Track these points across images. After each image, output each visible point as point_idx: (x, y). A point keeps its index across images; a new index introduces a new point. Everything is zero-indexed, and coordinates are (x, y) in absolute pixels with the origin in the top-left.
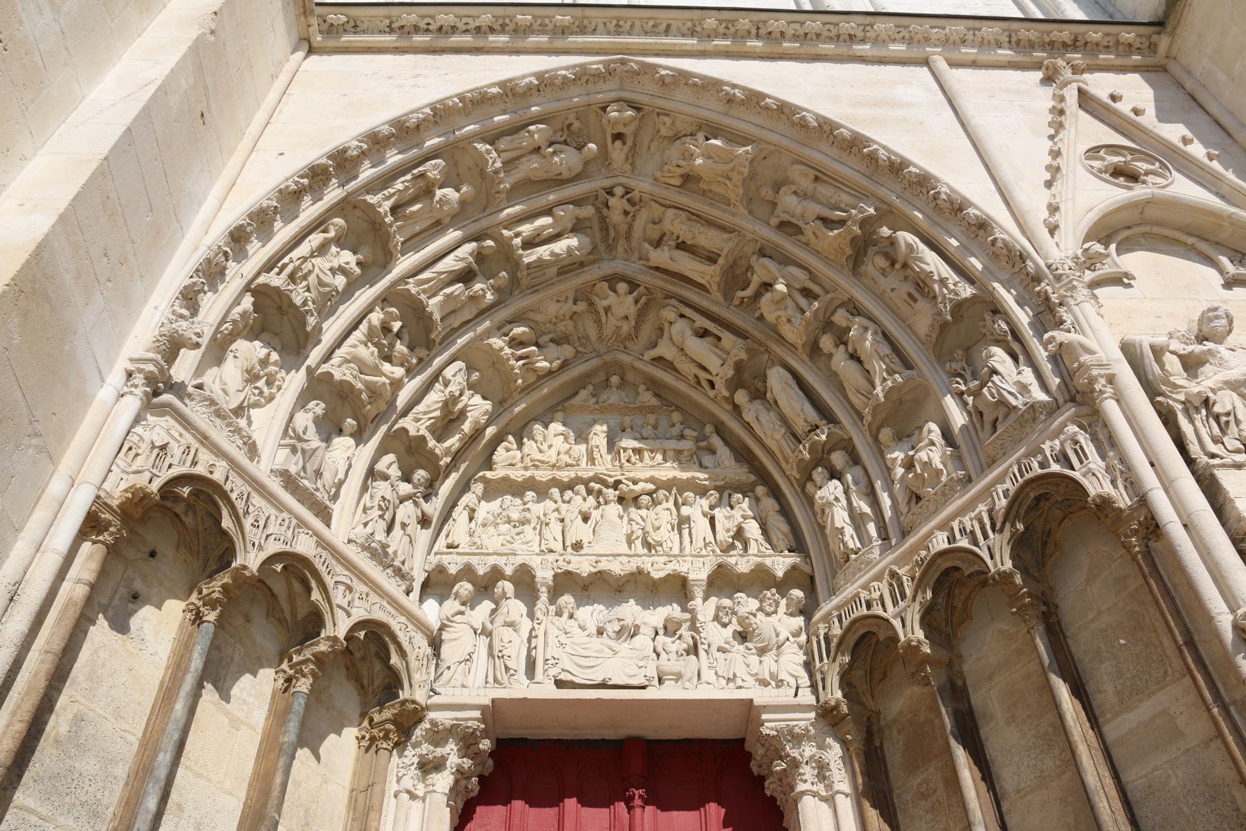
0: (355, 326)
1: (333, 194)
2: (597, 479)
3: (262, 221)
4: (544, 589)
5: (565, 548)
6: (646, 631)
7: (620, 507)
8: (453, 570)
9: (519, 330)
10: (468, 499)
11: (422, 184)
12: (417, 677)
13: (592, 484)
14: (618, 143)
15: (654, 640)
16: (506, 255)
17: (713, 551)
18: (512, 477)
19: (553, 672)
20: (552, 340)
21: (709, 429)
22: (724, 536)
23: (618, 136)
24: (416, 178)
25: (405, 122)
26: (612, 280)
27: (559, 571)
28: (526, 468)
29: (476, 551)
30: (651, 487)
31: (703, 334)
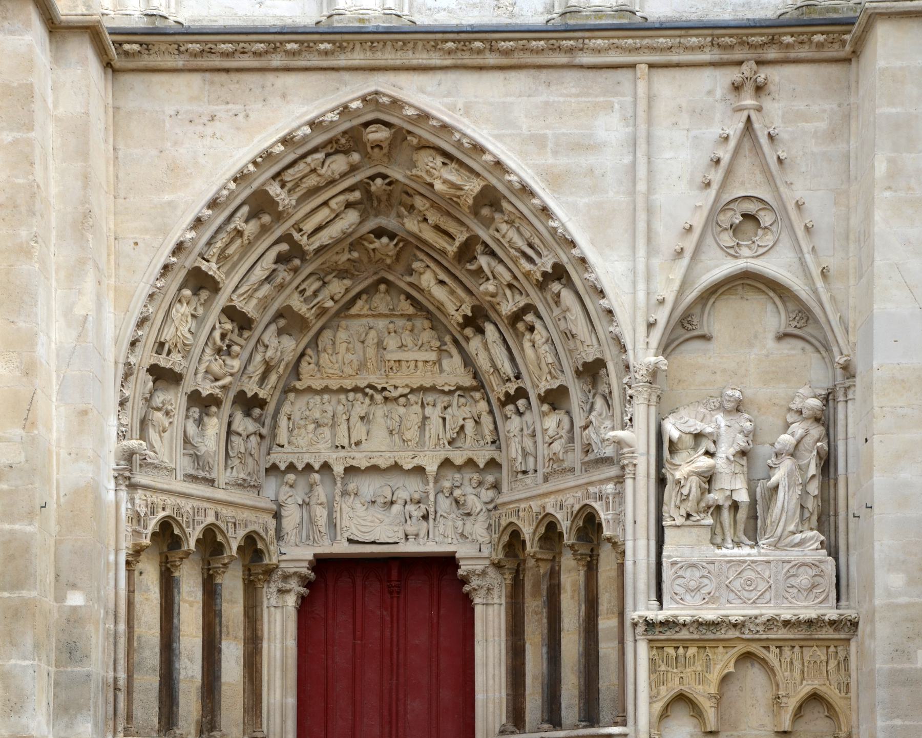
2: (370, 386)
4: (339, 479)
5: (350, 445)
6: (401, 502)
7: (385, 408)
8: (283, 467)
13: (367, 390)
15: (404, 506)
17: (444, 444)
18: (314, 387)
19: (346, 535)
21: (448, 339)
22: (451, 434)
26: (379, 233)
27: (348, 465)
29: (296, 450)
30: (407, 391)
31: (442, 282)
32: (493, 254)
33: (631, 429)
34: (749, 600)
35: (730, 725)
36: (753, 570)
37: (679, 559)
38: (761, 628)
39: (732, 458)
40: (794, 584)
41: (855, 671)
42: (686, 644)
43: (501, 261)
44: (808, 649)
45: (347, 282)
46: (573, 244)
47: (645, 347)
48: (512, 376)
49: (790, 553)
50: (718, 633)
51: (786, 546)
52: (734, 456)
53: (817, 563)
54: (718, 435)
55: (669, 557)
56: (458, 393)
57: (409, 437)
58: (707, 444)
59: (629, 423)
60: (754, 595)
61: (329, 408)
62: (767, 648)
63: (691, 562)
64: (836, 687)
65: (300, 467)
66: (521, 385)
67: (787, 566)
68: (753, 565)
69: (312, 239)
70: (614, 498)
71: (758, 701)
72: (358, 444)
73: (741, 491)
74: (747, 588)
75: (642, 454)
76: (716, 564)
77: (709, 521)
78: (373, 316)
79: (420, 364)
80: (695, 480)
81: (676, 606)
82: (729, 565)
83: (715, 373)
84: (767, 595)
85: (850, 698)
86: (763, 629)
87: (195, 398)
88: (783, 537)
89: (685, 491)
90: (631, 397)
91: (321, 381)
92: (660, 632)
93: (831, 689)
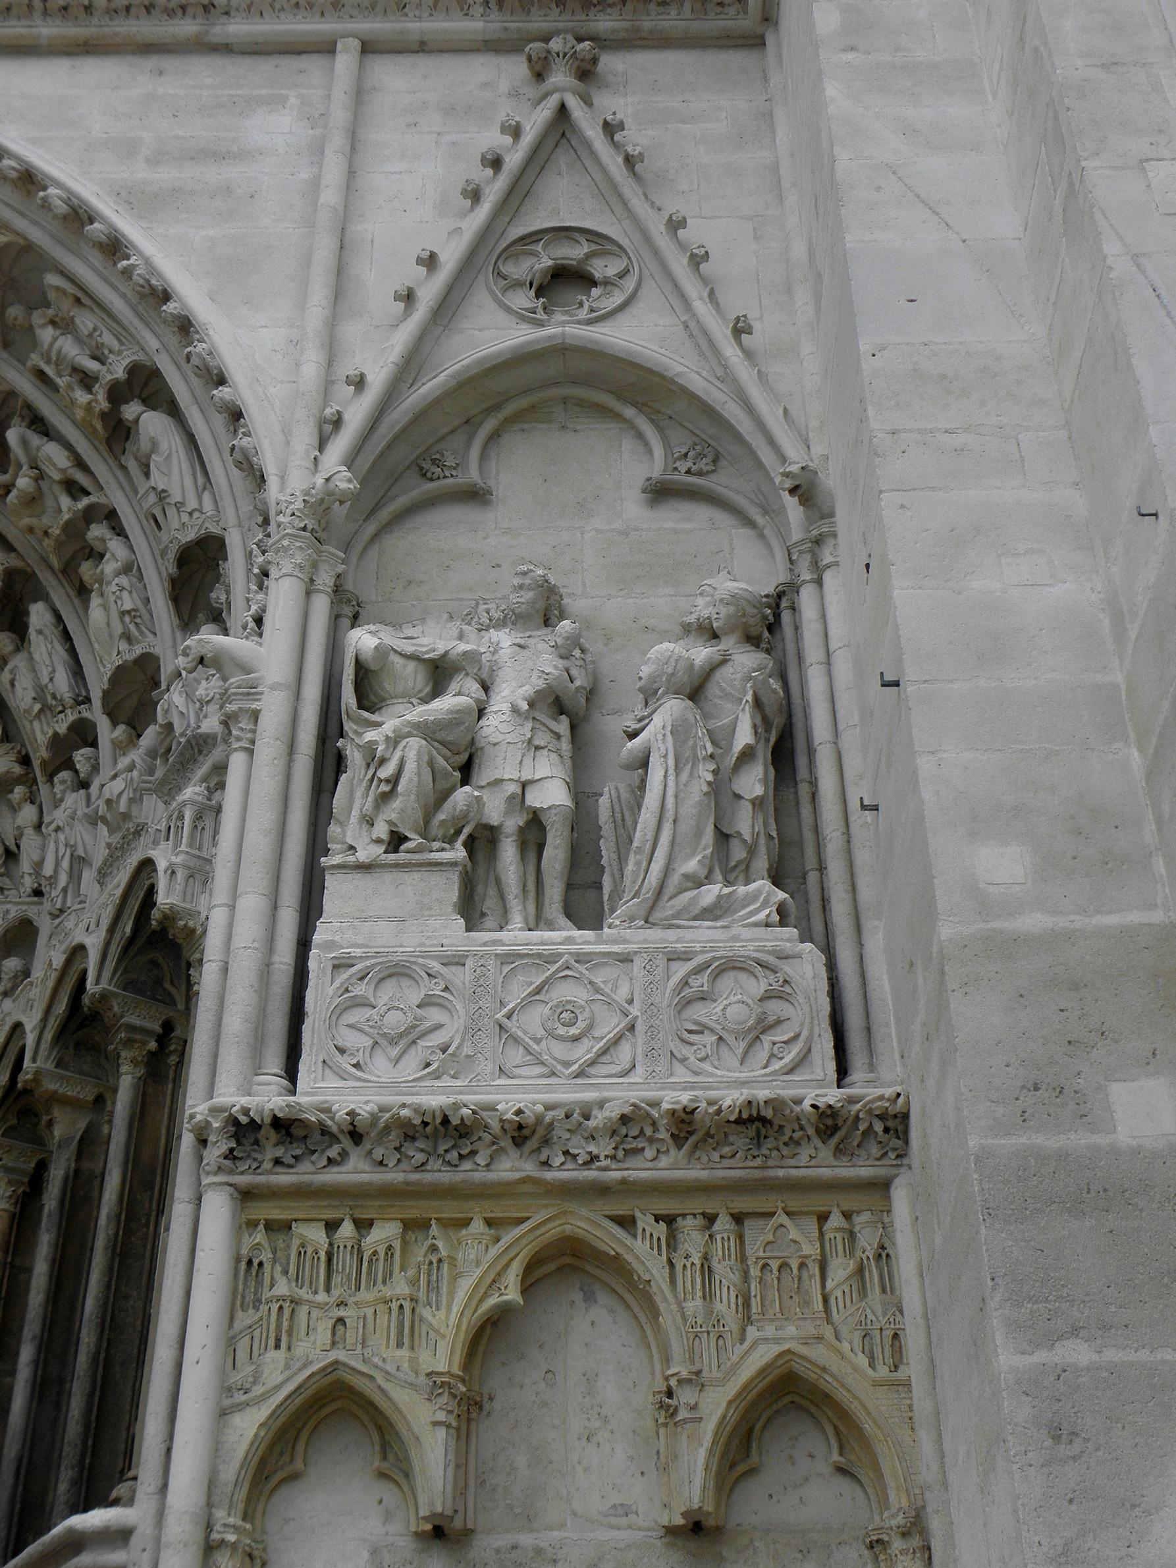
33: (256, 638)
34: (567, 1064)
35: (511, 1507)
37: (358, 952)
38: (603, 1148)
40: (704, 1020)
41: (915, 1281)
44: (760, 1222)
49: (689, 935)
50: (467, 1165)
51: (674, 917)
52: (531, 704)
53: (771, 960)
55: (330, 945)
59: (252, 624)
62: (627, 1223)
64: (858, 1349)
67: (681, 970)
70: (198, 817)
71: (606, 1420)
73: (546, 784)
74: (562, 1031)
76: (469, 963)
77: (458, 853)
80: (414, 747)
81: (341, 1083)
83: (499, 566)
84: (624, 1053)
85: (907, 1384)
86: (609, 1151)
88: (670, 889)
92: (277, 1162)
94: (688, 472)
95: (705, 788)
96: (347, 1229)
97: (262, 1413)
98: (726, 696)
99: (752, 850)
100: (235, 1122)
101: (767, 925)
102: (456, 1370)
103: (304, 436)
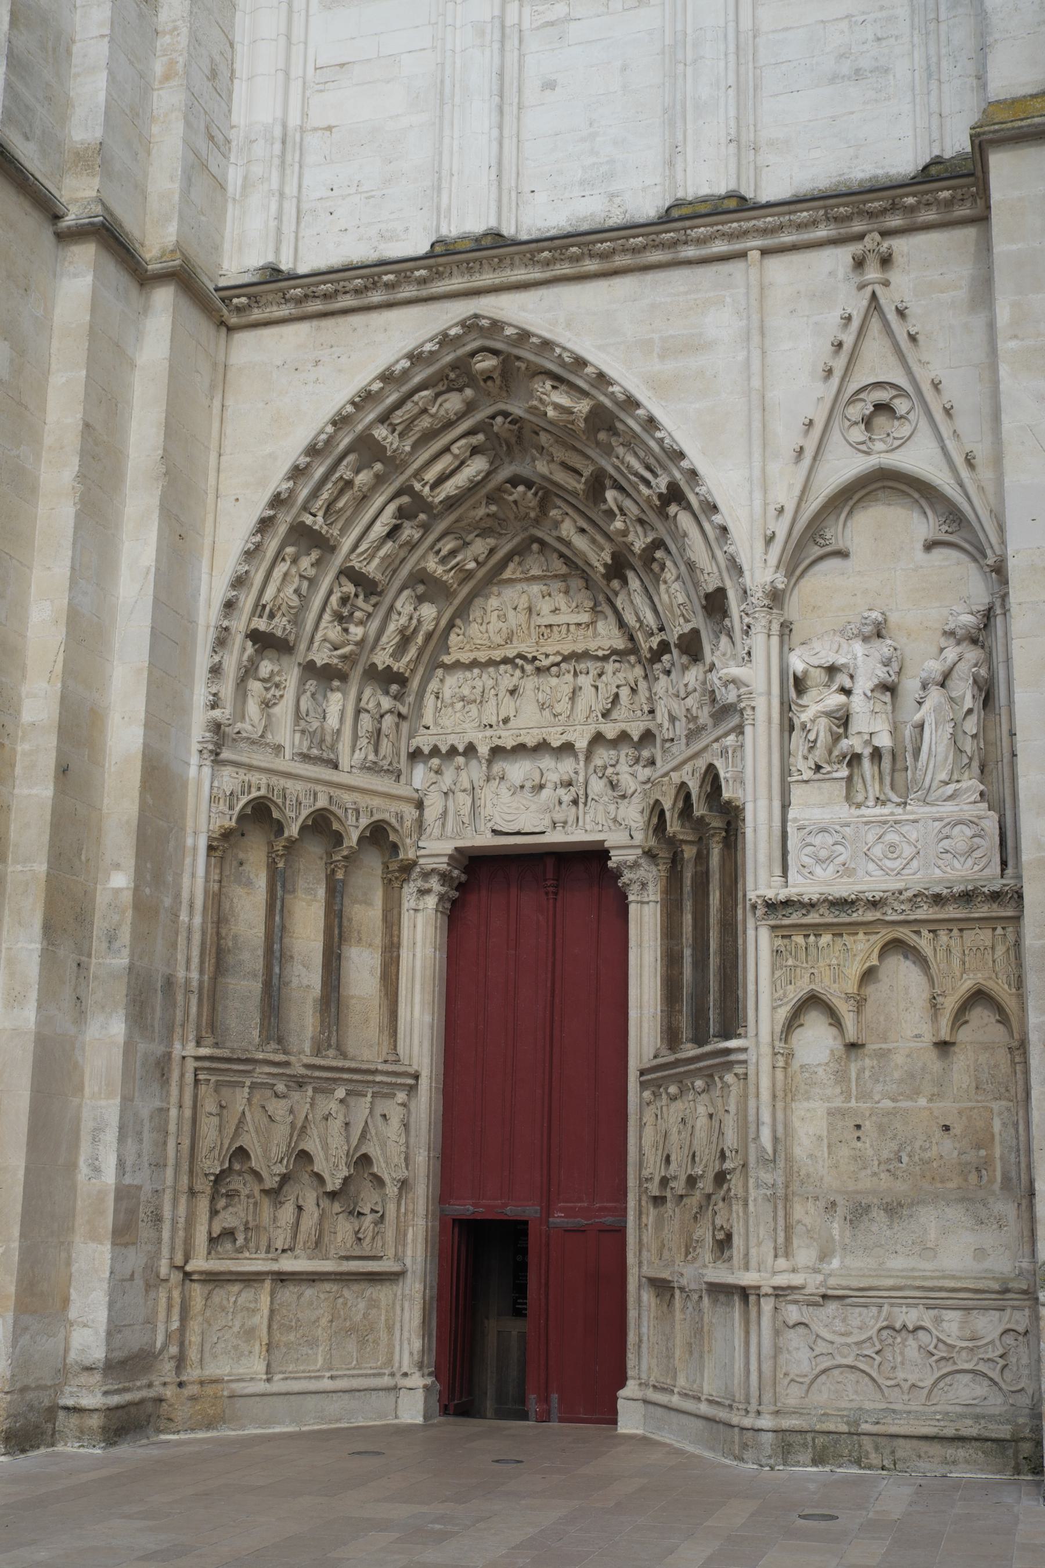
0: (323, 610)
1: (282, 529)
2: (520, 656)
3: (239, 582)
4: (483, 761)
8: (426, 750)
9: (448, 545)
10: (433, 685)
11: (341, 484)
12: (408, 841)
13: (518, 661)
14: (489, 383)
16: (420, 504)
18: (462, 660)
19: (489, 825)
20: (477, 536)
21: (601, 598)
22: (603, 704)
23: (490, 378)
24: (335, 483)
25: (316, 444)
26: (514, 481)
28: (472, 651)
30: (559, 658)
31: (583, 531)
32: (621, 488)
34: (892, 870)
36: (897, 832)
37: (806, 823)
39: (869, 694)
40: (947, 848)
42: (817, 929)
43: (629, 495)
44: (970, 931)
45: (491, 541)
46: (682, 455)
47: (762, 565)
48: (654, 627)
49: (942, 809)
50: (855, 915)
51: (937, 800)
54: (856, 667)
55: (795, 820)
56: (614, 657)
57: (559, 711)
58: (843, 679)
59: (746, 658)
60: (897, 864)
61: (479, 683)
62: (918, 933)
63: (822, 825)
65: (444, 749)
66: (665, 637)
68: (896, 826)
69: (438, 490)
70: (734, 752)
72: (506, 721)
73: (880, 734)
74: (890, 855)
75: (760, 694)
77: (844, 772)
78: (527, 579)
79: (572, 628)
80: (823, 722)
82: (867, 827)
84: (915, 864)
87: (310, 669)
88: (932, 791)
89: (812, 737)
90: (749, 627)
91: (469, 654)
93: (997, 983)
94: (946, 532)
95: (949, 736)
96: (812, 938)
97: (788, 1008)
98: (961, 679)
99: (971, 759)
100: (764, 901)
101: (975, 802)
102: (856, 991)
103: (760, 544)
